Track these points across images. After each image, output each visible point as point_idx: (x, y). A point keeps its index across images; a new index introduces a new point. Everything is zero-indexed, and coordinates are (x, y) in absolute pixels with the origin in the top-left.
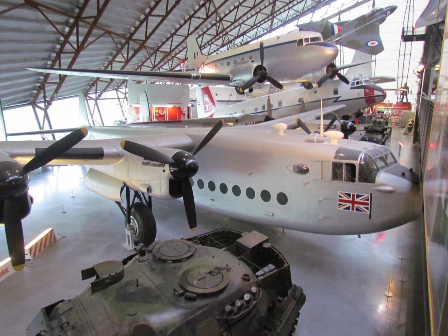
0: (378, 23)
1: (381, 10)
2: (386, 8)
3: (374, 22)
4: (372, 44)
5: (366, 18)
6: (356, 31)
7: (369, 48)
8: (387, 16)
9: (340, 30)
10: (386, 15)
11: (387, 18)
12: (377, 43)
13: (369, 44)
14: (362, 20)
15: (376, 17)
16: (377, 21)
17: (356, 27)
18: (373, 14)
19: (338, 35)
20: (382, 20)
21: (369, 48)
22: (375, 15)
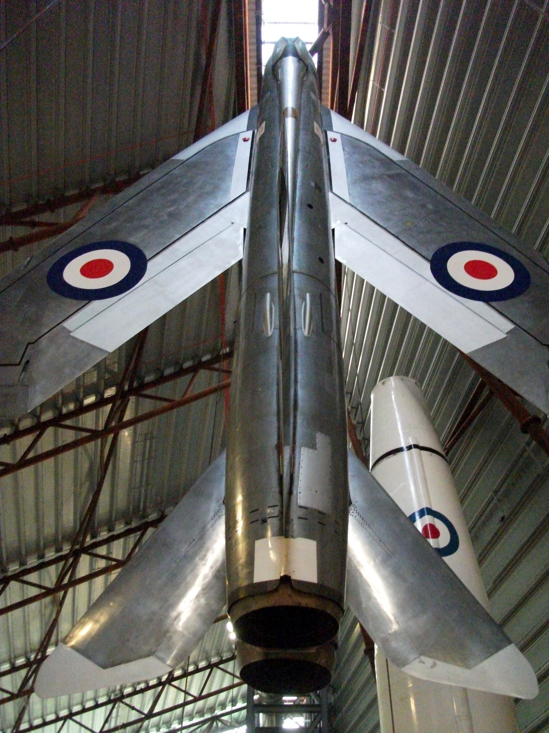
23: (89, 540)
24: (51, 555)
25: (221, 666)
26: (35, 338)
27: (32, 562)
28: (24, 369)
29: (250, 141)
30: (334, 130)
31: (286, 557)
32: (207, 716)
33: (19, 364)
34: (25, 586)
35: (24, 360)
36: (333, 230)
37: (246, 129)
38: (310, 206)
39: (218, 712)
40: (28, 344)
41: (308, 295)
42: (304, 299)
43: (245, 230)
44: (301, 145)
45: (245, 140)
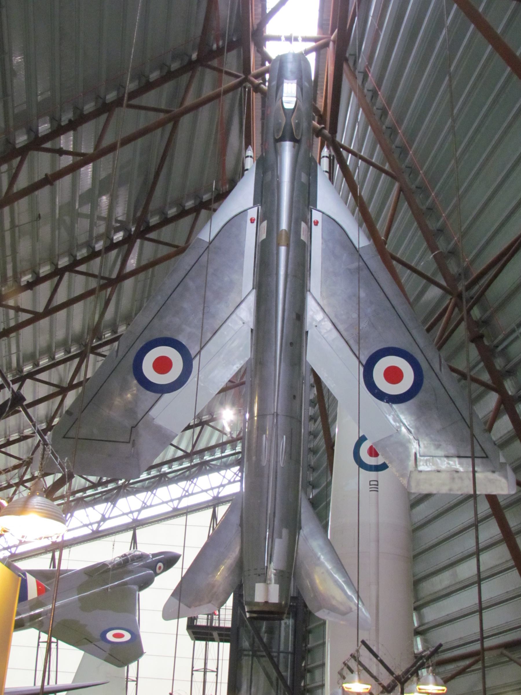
0: (136, 587)
1: (142, 557)
2: (154, 555)
3: (125, 583)
4: (115, 636)
5: (108, 570)
6: (80, 599)
7: (108, 647)
8: (157, 574)
9: (41, 591)
10: (155, 570)
11: (157, 579)
12: (127, 636)
13: (110, 636)
14: (98, 573)
15: (130, 572)
16: (134, 582)
17: (81, 588)
18: (125, 563)
19: (38, 603)
20: (145, 583)
21: (108, 647)
22: (130, 567)
23: (95, 343)
24: (60, 355)
25: (211, 424)
26: (136, 423)
27: (44, 362)
28: (133, 445)
29: (256, 222)
30: (318, 208)
31: (267, 591)
32: (197, 461)
33: (129, 442)
34: (37, 383)
35: (132, 439)
36: (307, 332)
37: (252, 205)
38: (291, 344)
39: (207, 458)
40: (132, 427)
41: (285, 436)
42: (283, 437)
43: (252, 330)
44: (289, 271)
45: (252, 221)
